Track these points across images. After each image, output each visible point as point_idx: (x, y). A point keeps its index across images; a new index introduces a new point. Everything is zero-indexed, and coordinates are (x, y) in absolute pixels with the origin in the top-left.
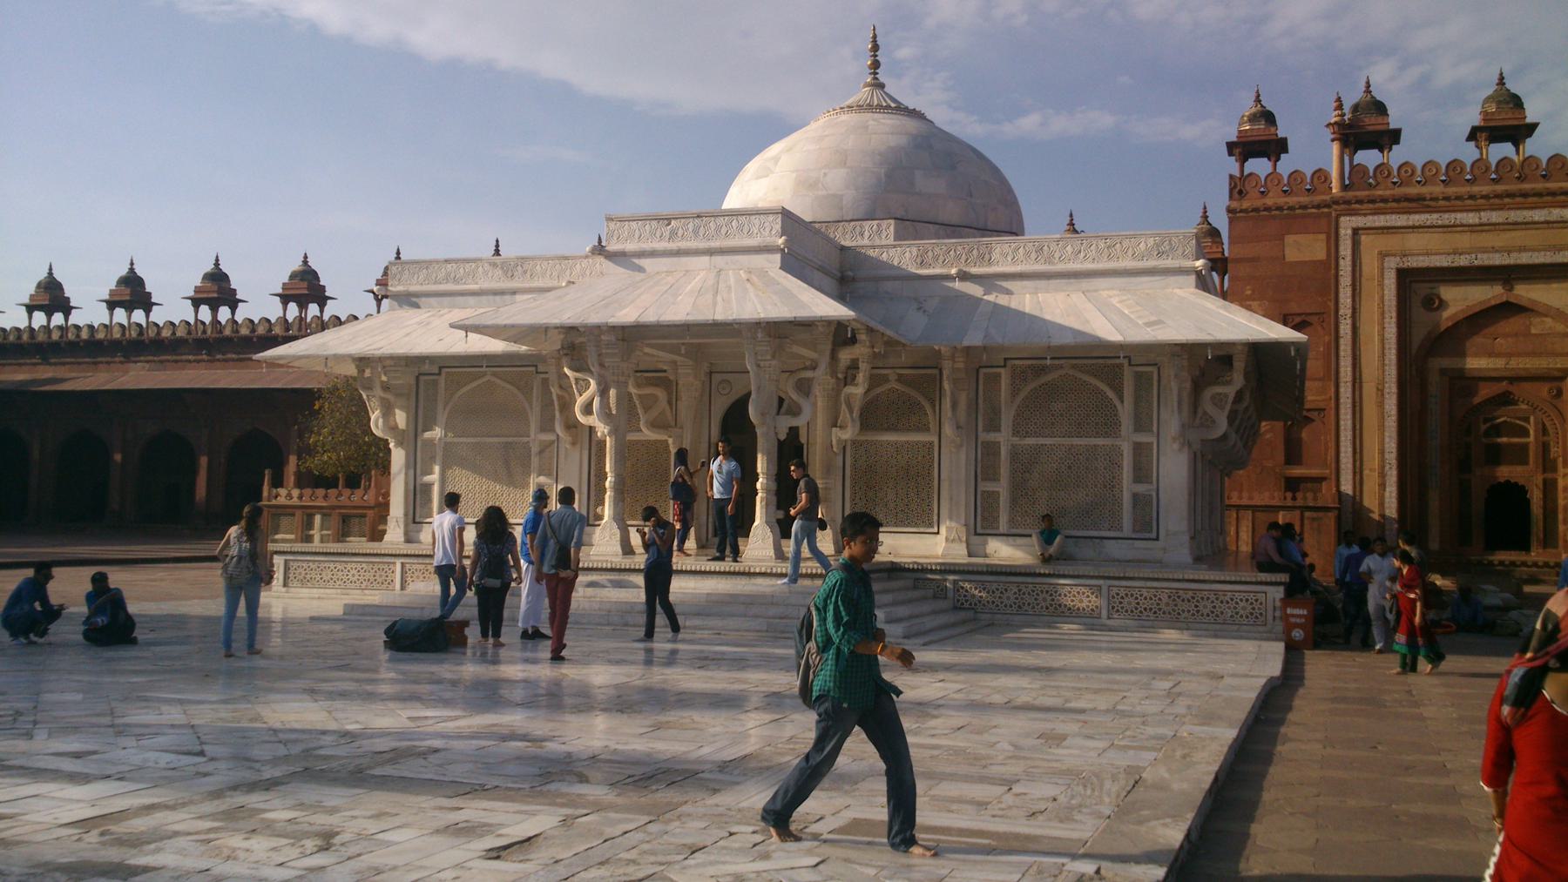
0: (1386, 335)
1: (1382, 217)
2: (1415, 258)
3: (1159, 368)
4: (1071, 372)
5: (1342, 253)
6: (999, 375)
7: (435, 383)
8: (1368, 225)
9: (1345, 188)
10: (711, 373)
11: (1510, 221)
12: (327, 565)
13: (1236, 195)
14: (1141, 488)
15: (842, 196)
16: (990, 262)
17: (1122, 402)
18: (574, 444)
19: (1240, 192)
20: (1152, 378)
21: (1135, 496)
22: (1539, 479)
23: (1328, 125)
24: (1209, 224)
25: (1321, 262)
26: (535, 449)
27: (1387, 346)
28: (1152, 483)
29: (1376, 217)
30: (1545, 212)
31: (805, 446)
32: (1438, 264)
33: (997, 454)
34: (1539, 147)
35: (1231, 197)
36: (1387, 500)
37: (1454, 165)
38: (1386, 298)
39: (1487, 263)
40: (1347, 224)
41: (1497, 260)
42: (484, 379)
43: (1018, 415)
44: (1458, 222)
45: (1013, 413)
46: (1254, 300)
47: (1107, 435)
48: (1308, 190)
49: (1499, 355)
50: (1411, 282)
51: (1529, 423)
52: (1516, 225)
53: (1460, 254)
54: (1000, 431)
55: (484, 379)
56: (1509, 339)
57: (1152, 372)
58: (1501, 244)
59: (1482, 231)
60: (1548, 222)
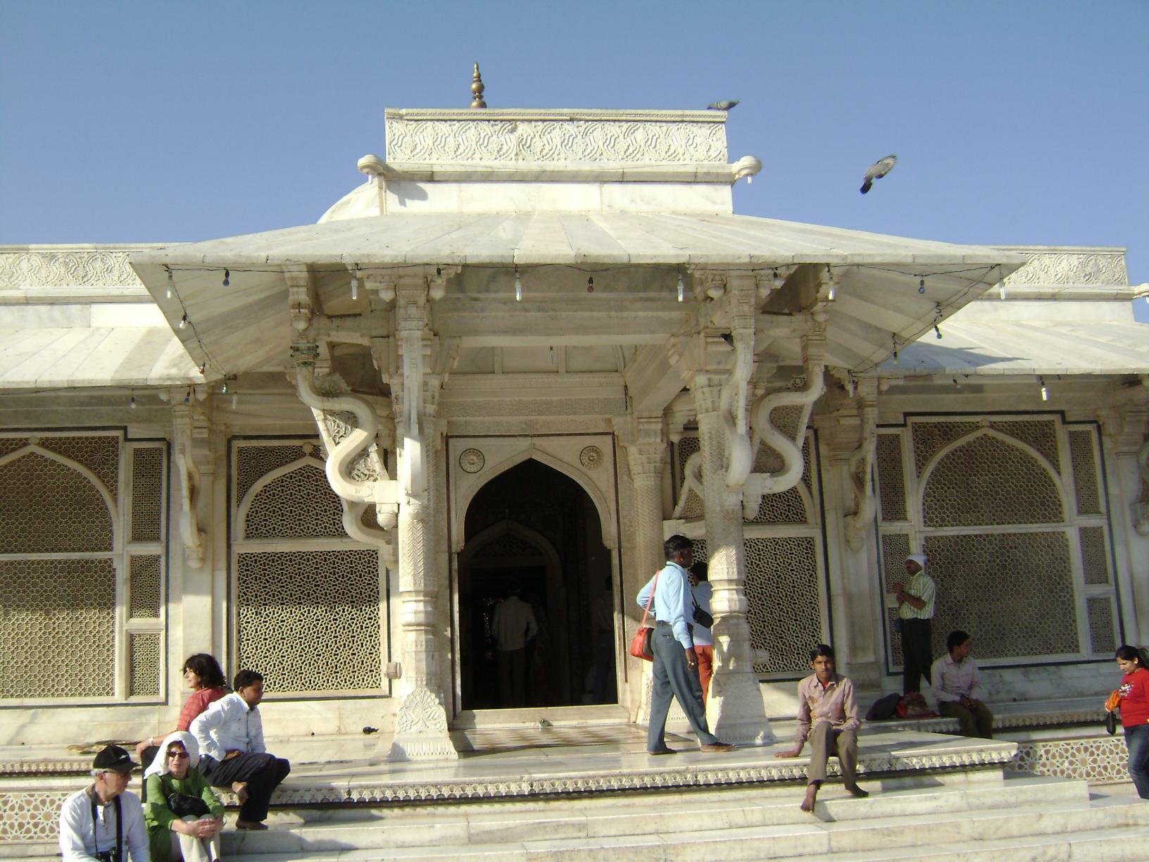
3: (1099, 429)
4: (991, 433)
14: (1097, 590)
17: (1059, 473)
18: (203, 560)
21: (1091, 602)
26: (122, 573)
28: (1107, 582)
31: (615, 554)
43: (927, 495)
45: (922, 491)
47: (1046, 519)
54: (905, 519)
57: (1089, 433)
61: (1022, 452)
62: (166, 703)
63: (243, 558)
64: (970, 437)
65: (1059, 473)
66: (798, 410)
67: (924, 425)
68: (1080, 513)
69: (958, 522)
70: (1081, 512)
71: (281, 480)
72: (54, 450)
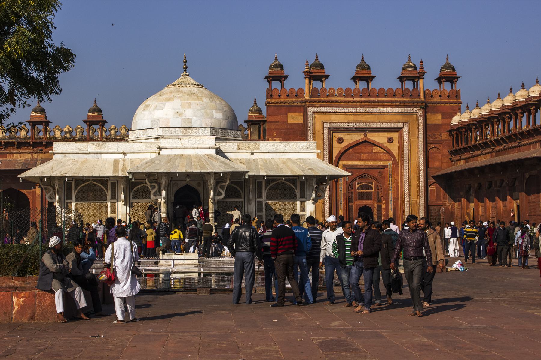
0: (325, 152)
1: (323, 108)
2: (335, 124)
3: (307, 180)
5: (309, 121)
6: (262, 181)
7: (71, 183)
8: (318, 111)
9: (310, 96)
10: (171, 181)
11: (366, 111)
13: (270, 97)
15: (191, 119)
16: (259, 149)
19: (271, 96)
20: (305, 183)
22: (376, 205)
23: (304, 72)
24: (257, 106)
25: (301, 124)
27: (325, 157)
29: (321, 108)
32: (343, 127)
33: (262, 205)
34: (375, 85)
35: (267, 98)
36: (325, 214)
37: (348, 89)
38: (325, 138)
39: (359, 126)
40: (311, 110)
41: (362, 125)
43: (267, 193)
44: (349, 111)
45: (266, 192)
46: (277, 138)
48: (296, 96)
49: (363, 160)
50: (333, 132)
51: (372, 185)
52: (369, 113)
53: (350, 123)
54: (262, 198)
56: (366, 155)
58: (364, 120)
59: (357, 115)
60: (379, 112)
61: (289, 185)
64: (278, 182)
66: (225, 185)
71: (139, 188)
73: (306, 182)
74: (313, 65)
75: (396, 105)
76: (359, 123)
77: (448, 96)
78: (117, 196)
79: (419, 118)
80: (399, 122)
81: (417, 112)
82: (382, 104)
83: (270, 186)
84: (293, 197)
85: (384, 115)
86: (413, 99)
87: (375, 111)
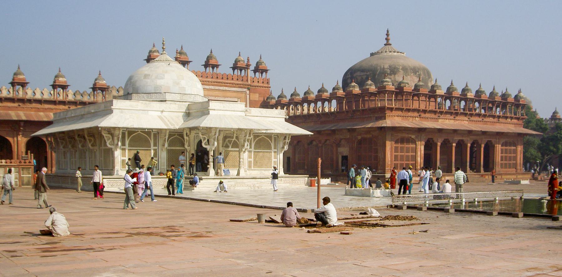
4: (264, 137)
12: (118, 181)
17: (272, 142)
30: (222, 87)
42: (138, 132)
43: (254, 145)
47: (269, 150)
55: (138, 132)
59: (210, 91)
60: (223, 90)
62: (158, 170)
63: (168, 149)
64: (261, 137)
65: (272, 142)
66: (249, 139)
67: (255, 135)
68: (274, 149)
69: (258, 149)
70: (274, 149)
71: (172, 139)
72: (142, 133)
73: (277, 138)
74: (180, 53)
75: (233, 86)
76: (210, 96)
77: (263, 82)
78: (157, 143)
79: (247, 96)
80: (235, 97)
81: (246, 92)
82: (225, 84)
83: (257, 140)
84: (270, 148)
85: (226, 92)
86: (244, 83)
87: (221, 89)
